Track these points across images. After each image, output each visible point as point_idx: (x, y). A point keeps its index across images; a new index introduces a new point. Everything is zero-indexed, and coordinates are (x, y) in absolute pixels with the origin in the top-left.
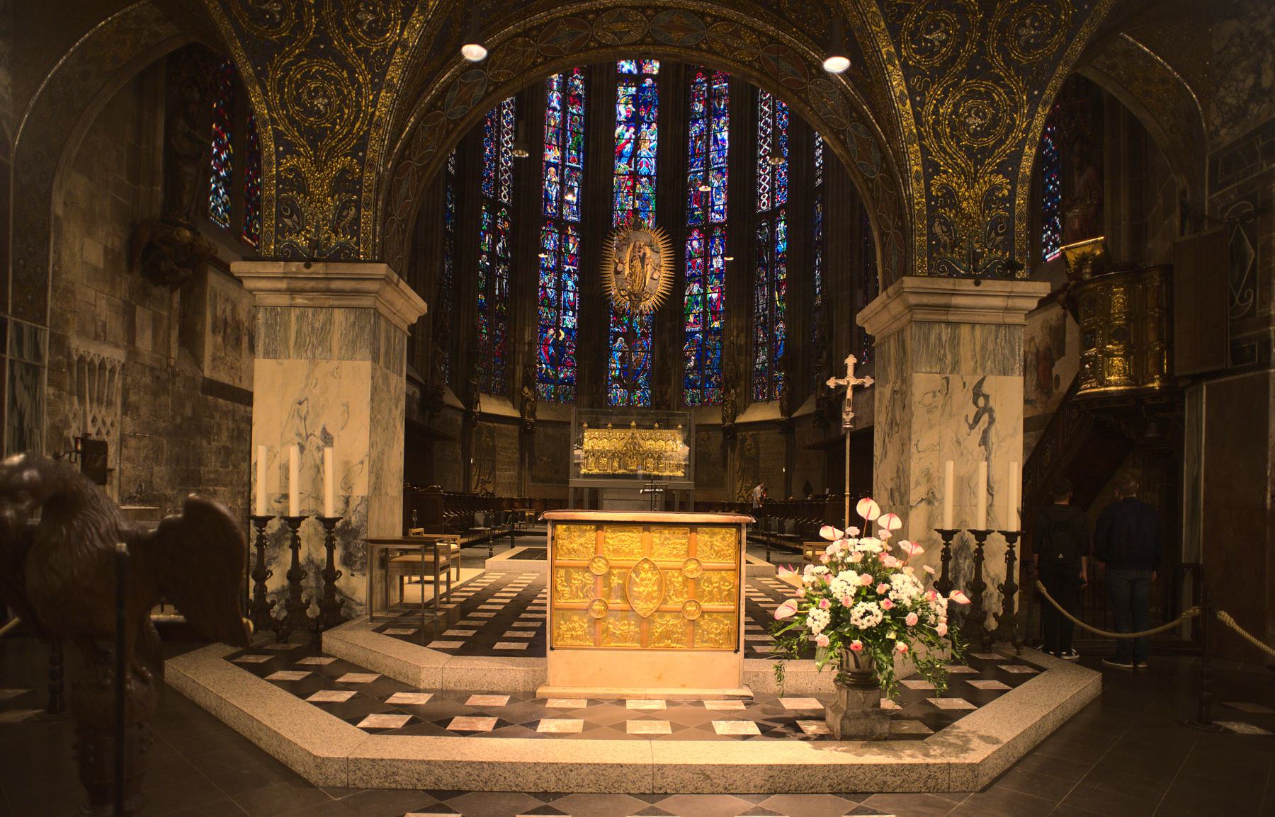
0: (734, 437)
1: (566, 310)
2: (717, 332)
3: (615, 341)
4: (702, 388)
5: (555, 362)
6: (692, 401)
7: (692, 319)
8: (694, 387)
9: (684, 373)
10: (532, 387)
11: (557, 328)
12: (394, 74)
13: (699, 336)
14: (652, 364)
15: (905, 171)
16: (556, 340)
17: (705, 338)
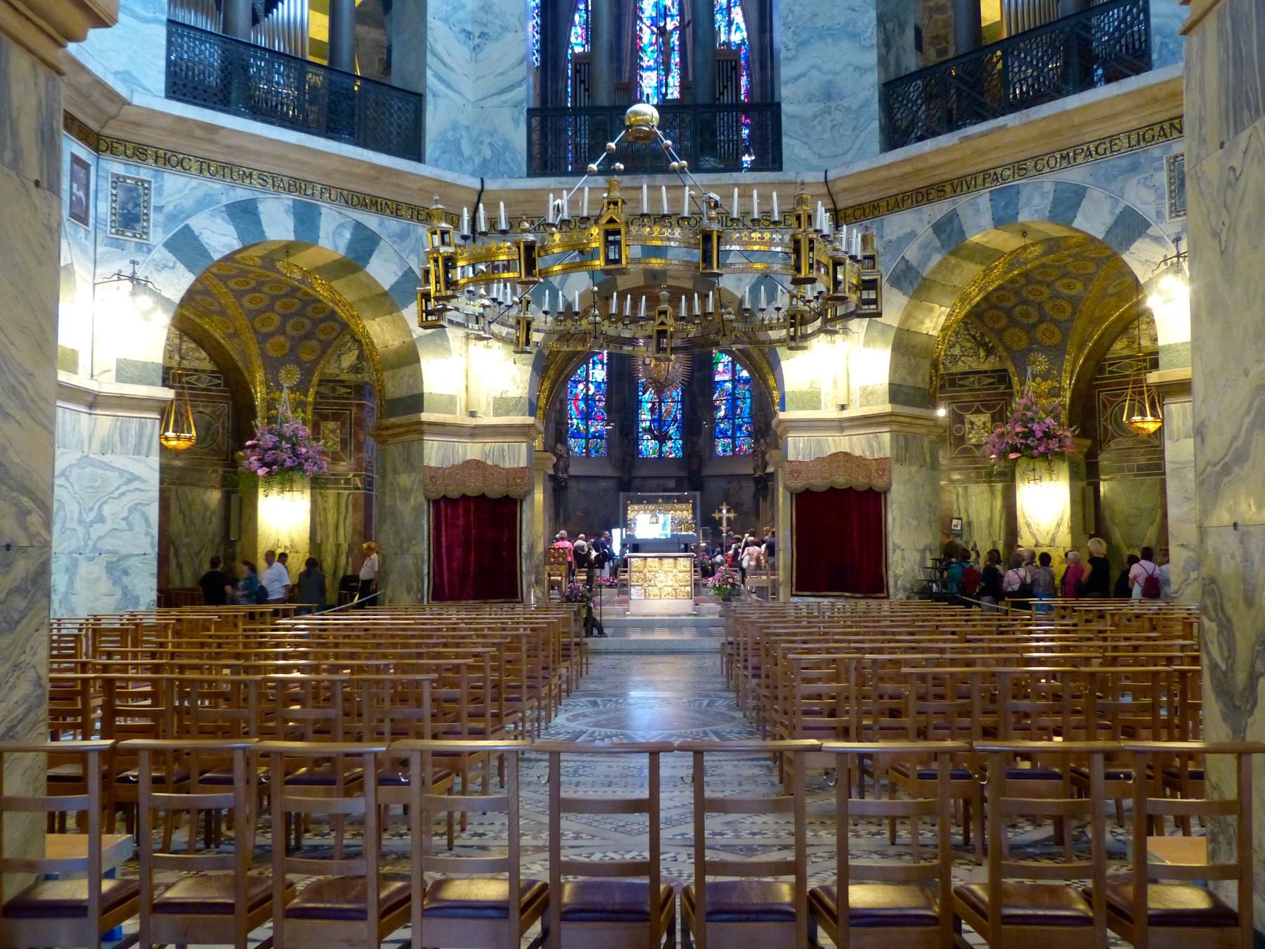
0: (766, 488)
1: (594, 363)
2: (746, 381)
3: (644, 393)
4: (733, 438)
5: (586, 416)
6: (724, 451)
7: (720, 367)
8: (726, 437)
9: (713, 422)
10: (564, 443)
11: (587, 381)
12: (551, 373)
13: (729, 385)
14: (683, 414)
15: (773, 402)
16: (587, 394)
17: (734, 388)
